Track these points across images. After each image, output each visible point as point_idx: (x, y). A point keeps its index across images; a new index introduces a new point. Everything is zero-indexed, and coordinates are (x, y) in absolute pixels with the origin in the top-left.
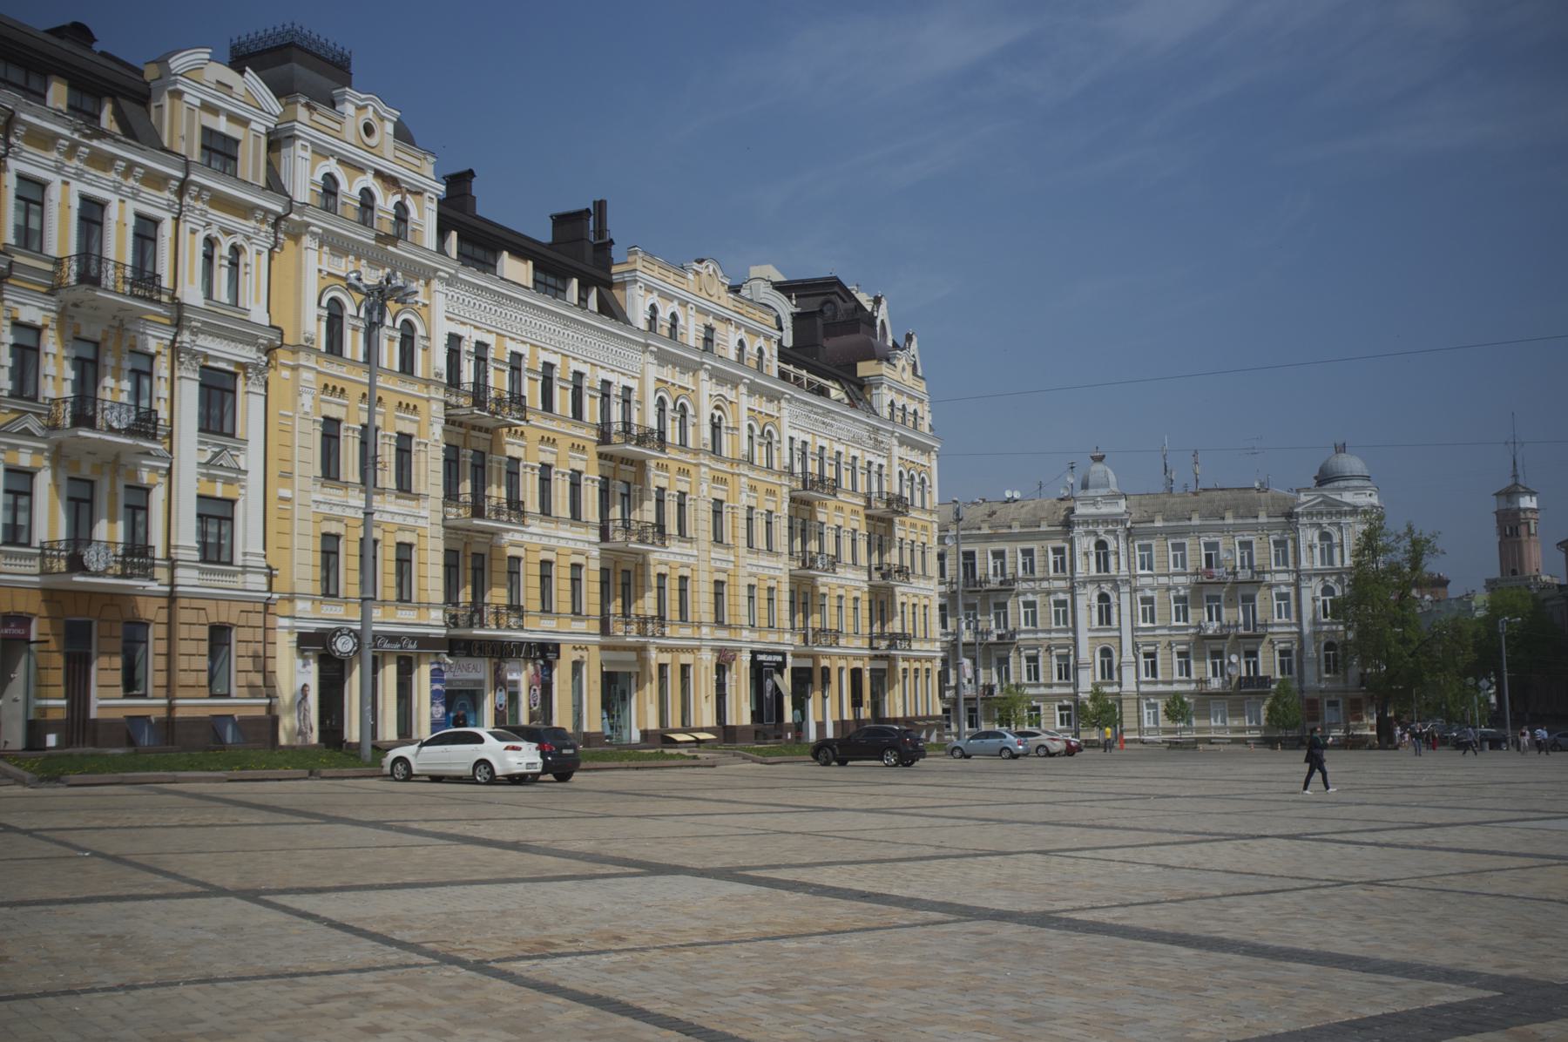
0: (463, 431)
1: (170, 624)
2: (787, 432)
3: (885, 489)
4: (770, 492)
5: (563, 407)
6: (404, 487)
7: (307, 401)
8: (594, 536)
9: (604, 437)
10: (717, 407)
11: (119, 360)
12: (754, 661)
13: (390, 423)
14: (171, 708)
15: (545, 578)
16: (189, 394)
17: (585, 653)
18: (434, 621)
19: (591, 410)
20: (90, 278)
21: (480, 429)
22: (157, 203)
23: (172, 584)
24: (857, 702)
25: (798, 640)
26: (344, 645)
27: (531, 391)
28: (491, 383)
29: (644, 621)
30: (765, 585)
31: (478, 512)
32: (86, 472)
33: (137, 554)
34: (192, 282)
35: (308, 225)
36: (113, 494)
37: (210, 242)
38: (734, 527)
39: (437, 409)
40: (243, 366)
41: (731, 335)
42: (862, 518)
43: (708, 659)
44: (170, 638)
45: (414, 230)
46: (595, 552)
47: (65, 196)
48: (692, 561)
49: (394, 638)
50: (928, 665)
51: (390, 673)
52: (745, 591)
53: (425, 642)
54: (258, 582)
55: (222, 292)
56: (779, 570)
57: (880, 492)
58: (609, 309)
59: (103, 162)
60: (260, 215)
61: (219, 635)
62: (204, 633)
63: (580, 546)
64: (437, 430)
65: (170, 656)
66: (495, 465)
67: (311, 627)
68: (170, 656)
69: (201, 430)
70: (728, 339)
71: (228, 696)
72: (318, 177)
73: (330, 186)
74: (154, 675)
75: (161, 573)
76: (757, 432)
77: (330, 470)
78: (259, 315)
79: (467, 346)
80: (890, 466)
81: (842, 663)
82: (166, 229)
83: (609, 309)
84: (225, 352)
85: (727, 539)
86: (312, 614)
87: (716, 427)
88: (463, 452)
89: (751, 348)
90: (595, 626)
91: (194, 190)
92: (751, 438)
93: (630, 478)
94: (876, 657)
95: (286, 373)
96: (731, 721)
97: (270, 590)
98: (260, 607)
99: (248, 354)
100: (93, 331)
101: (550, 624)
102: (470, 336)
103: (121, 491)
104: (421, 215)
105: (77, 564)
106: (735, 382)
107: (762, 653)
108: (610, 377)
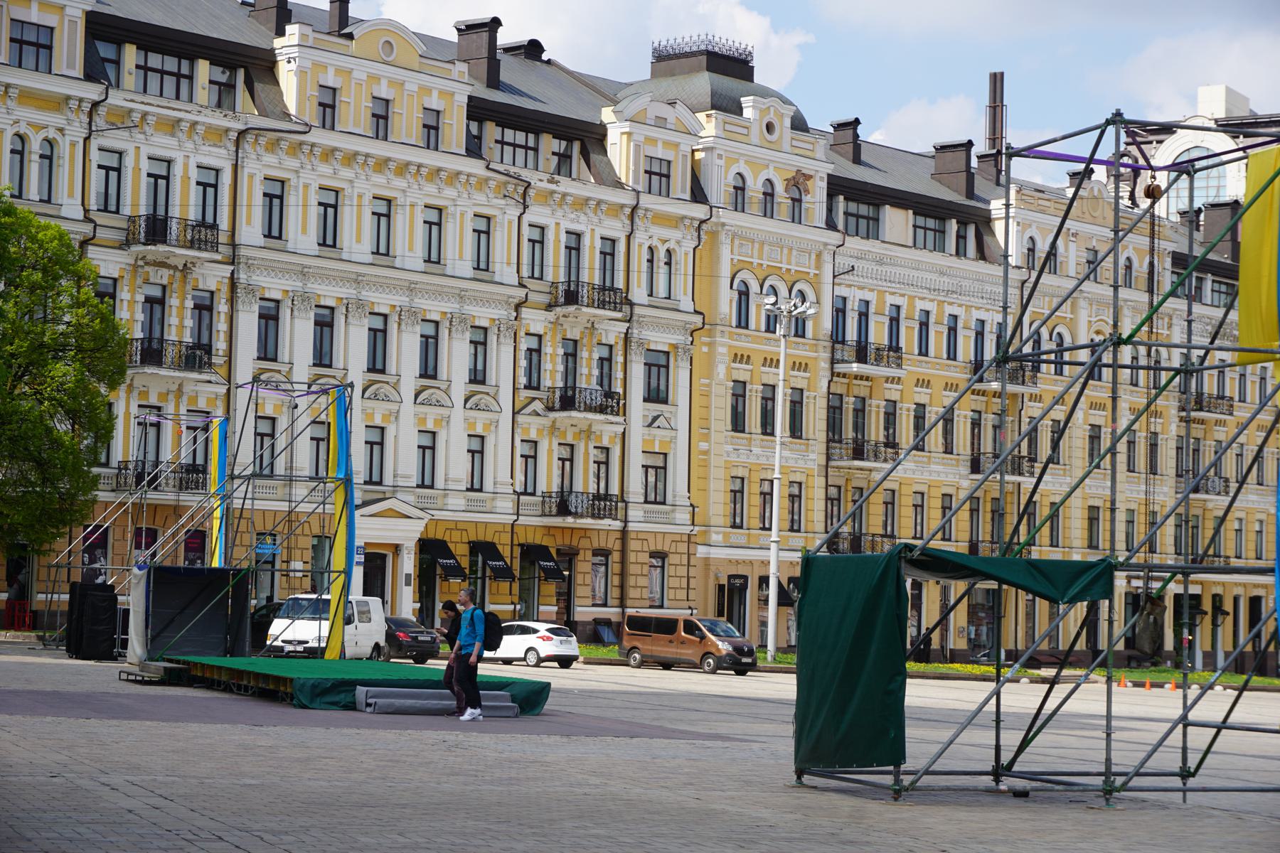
0: (845, 381)
1: (623, 552)
7: (721, 370)
11: (591, 352)
21: (862, 378)
23: (626, 522)
28: (871, 339)
32: (570, 440)
34: (639, 286)
35: (723, 225)
36: (587, 453)
40: (676, 347)
44: (623, 561)
45: (807, 210)
54: (683, 516)
55: (661, 290)
60: (687, 222)
66: (874, 409)
69: (645, 400)
71: (661, 607)
75: (620, 514)
77: (738, 423)
78: (686, 304)
82: (621, 248)
88: (845, 399)
91: (640, 212)
95: (705, 349)
97: (693, 524)
98: (685, 538)
100: (574, 334)
102: (855, 298)
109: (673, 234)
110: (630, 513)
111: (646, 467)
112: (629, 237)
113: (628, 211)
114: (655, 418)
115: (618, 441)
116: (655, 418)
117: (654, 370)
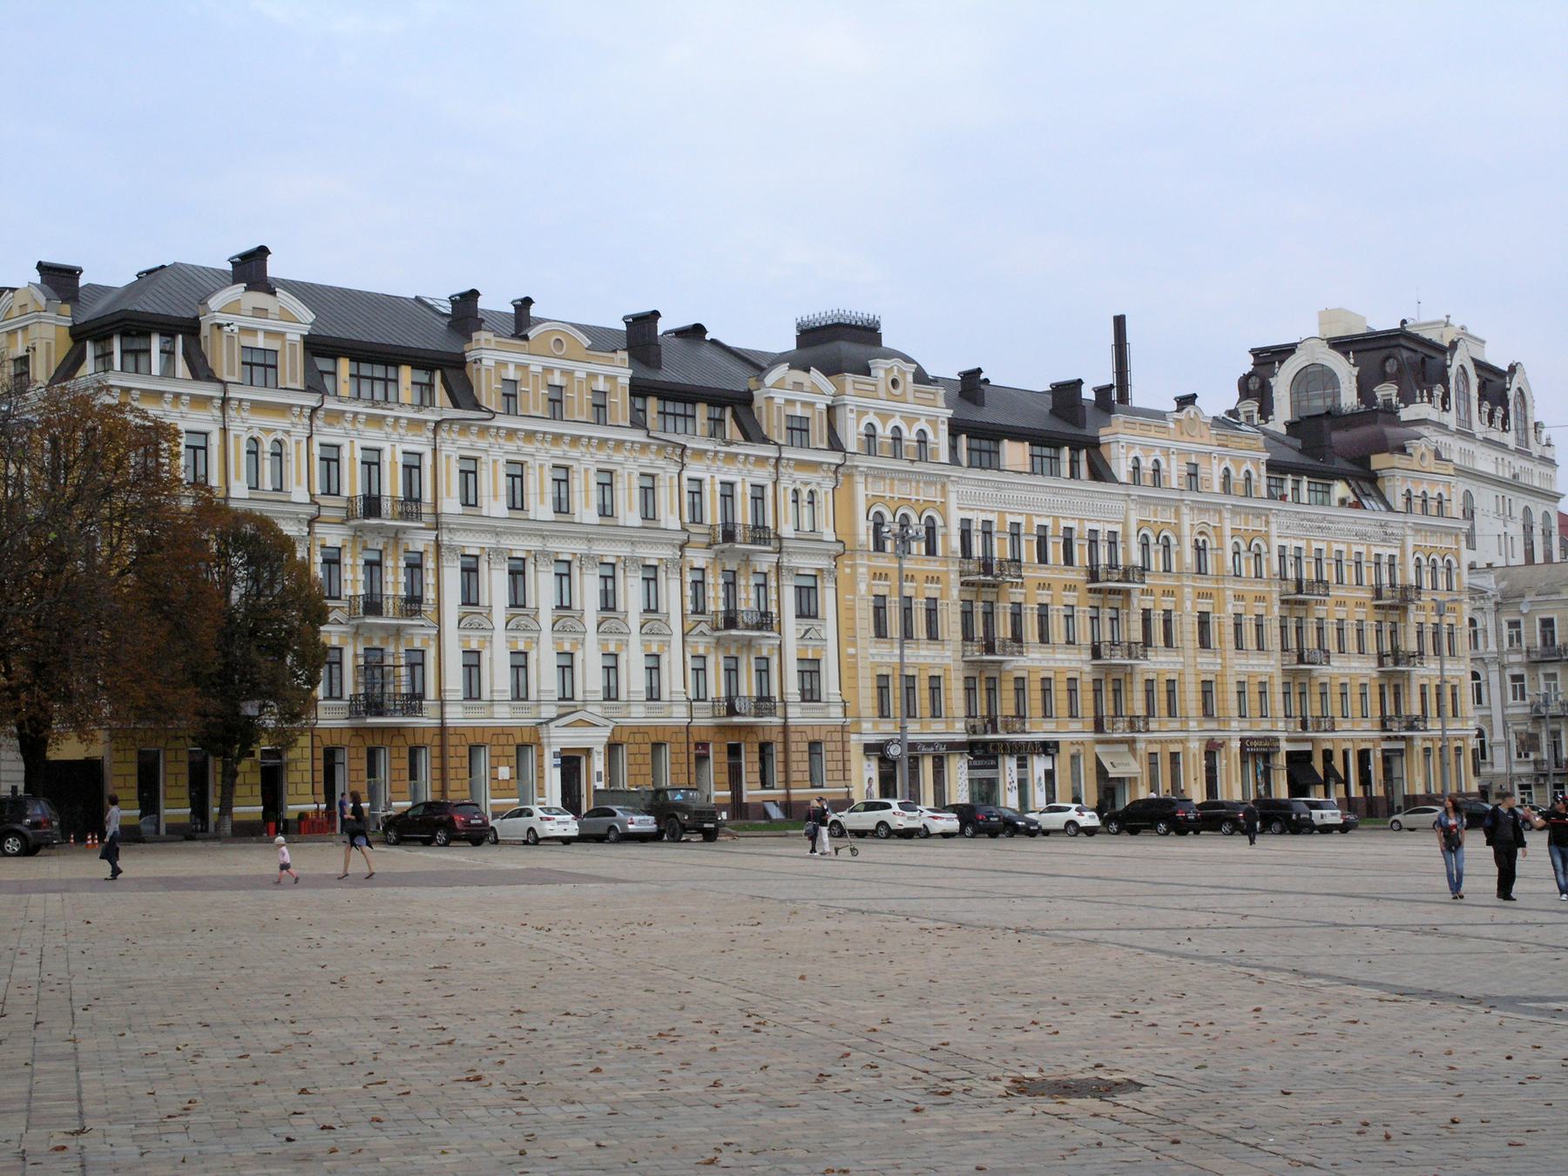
2: (1276, 543)
3: (1398, 581)
4: (1260, 599)
5: (1056, 556)
6: (932, 635)
8: (1087, 655)
9: (1093, 575)
10: (1201, 533)
12: (1243, 748)
13: (920, 593)
14: (788, 795)
15: (1072, 691)
16: (789, 596)
17: (1081, 748)
18: (958, 731)
19: (1081, 555)
20: (729, 536)
22: (763, 475)
23: (786, 718)
24: (1365, 779)
25: (1294, 725)
26: (894, 751)
27: (1028, 551)
29: (1132, 722)
30: (1255, 681)
31: (990, 648)
33: (764, 702)
37: (796, 492)
38: (1222, 630)
39: (954, 579)
40: (821, 570)
41: (1215, 467)
42: (1369, 609)
43: (1196, 747)
46: (1088, 668)
47: (713, 484)
48: (1179, 667)
49: (929, 745)
50: (1460, 744)
51: (927, 767)
52: (1234, 688)
53: (953, 746)
55: (806, 526)
56: (1269, 666)
57: (1392, 585)
58: (1100, 472)
59: (732, 457)
61: (814, 747)
62: (805, 747)
63: (1074, 664)
64: (955, 593)
65: (786, 763)
67: (872, 739)
68: (786, 763)
70: (1213, 473)
72: (862, 429)
73: (871, 435)
74: (778, 777)
76: (1243, 547)
79: (976, 526)
80: (1403, 554)
81: (1348, 745)
82: (769, 492)
83: (1100, 472)
84: (808, 564)
85: (1214, 643)
86: (873, 730)
87: (1200, 550)
89: (1238, 476)
90: (1090, 723)
91: (784, 462)
92: (1236, 553)
93: (1118, 604)
94: (1389, 739)
96: (1222, 796)
99: (824, 563)
101: (1050, 725)
103: (753, 661)
104: (936, 436)
105: (731, 711)
106: (1218, 509)
107: (1252, 739)
108: (1095, 526)
109: (813, 477)
110: (790, 710)
111: (801, 672)
112: (775, 483)
113: (773, 461)
114: (807, 631)
115: (776, 652)
116: (807, 631)
117: (804, 592)
